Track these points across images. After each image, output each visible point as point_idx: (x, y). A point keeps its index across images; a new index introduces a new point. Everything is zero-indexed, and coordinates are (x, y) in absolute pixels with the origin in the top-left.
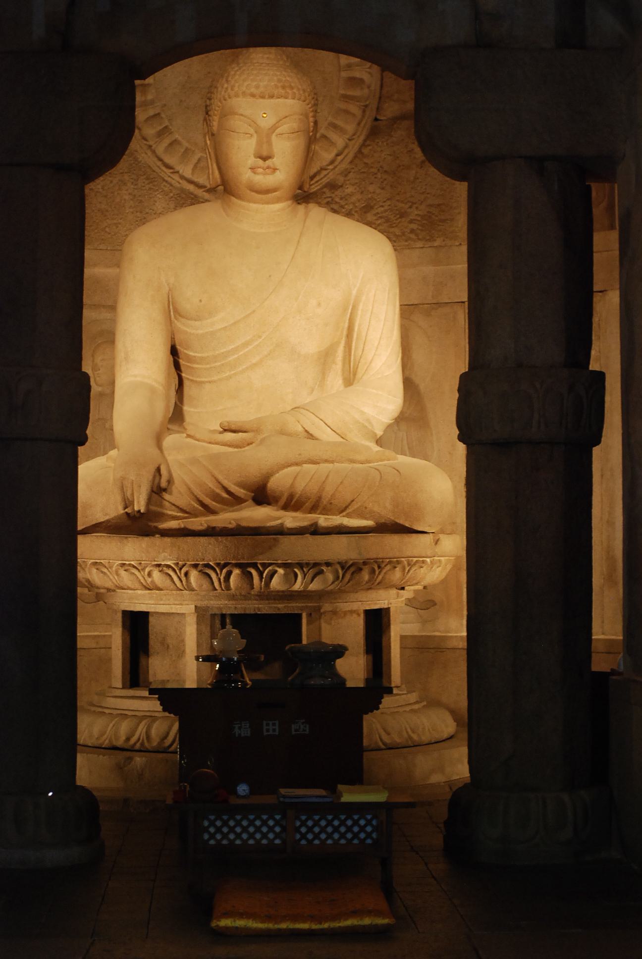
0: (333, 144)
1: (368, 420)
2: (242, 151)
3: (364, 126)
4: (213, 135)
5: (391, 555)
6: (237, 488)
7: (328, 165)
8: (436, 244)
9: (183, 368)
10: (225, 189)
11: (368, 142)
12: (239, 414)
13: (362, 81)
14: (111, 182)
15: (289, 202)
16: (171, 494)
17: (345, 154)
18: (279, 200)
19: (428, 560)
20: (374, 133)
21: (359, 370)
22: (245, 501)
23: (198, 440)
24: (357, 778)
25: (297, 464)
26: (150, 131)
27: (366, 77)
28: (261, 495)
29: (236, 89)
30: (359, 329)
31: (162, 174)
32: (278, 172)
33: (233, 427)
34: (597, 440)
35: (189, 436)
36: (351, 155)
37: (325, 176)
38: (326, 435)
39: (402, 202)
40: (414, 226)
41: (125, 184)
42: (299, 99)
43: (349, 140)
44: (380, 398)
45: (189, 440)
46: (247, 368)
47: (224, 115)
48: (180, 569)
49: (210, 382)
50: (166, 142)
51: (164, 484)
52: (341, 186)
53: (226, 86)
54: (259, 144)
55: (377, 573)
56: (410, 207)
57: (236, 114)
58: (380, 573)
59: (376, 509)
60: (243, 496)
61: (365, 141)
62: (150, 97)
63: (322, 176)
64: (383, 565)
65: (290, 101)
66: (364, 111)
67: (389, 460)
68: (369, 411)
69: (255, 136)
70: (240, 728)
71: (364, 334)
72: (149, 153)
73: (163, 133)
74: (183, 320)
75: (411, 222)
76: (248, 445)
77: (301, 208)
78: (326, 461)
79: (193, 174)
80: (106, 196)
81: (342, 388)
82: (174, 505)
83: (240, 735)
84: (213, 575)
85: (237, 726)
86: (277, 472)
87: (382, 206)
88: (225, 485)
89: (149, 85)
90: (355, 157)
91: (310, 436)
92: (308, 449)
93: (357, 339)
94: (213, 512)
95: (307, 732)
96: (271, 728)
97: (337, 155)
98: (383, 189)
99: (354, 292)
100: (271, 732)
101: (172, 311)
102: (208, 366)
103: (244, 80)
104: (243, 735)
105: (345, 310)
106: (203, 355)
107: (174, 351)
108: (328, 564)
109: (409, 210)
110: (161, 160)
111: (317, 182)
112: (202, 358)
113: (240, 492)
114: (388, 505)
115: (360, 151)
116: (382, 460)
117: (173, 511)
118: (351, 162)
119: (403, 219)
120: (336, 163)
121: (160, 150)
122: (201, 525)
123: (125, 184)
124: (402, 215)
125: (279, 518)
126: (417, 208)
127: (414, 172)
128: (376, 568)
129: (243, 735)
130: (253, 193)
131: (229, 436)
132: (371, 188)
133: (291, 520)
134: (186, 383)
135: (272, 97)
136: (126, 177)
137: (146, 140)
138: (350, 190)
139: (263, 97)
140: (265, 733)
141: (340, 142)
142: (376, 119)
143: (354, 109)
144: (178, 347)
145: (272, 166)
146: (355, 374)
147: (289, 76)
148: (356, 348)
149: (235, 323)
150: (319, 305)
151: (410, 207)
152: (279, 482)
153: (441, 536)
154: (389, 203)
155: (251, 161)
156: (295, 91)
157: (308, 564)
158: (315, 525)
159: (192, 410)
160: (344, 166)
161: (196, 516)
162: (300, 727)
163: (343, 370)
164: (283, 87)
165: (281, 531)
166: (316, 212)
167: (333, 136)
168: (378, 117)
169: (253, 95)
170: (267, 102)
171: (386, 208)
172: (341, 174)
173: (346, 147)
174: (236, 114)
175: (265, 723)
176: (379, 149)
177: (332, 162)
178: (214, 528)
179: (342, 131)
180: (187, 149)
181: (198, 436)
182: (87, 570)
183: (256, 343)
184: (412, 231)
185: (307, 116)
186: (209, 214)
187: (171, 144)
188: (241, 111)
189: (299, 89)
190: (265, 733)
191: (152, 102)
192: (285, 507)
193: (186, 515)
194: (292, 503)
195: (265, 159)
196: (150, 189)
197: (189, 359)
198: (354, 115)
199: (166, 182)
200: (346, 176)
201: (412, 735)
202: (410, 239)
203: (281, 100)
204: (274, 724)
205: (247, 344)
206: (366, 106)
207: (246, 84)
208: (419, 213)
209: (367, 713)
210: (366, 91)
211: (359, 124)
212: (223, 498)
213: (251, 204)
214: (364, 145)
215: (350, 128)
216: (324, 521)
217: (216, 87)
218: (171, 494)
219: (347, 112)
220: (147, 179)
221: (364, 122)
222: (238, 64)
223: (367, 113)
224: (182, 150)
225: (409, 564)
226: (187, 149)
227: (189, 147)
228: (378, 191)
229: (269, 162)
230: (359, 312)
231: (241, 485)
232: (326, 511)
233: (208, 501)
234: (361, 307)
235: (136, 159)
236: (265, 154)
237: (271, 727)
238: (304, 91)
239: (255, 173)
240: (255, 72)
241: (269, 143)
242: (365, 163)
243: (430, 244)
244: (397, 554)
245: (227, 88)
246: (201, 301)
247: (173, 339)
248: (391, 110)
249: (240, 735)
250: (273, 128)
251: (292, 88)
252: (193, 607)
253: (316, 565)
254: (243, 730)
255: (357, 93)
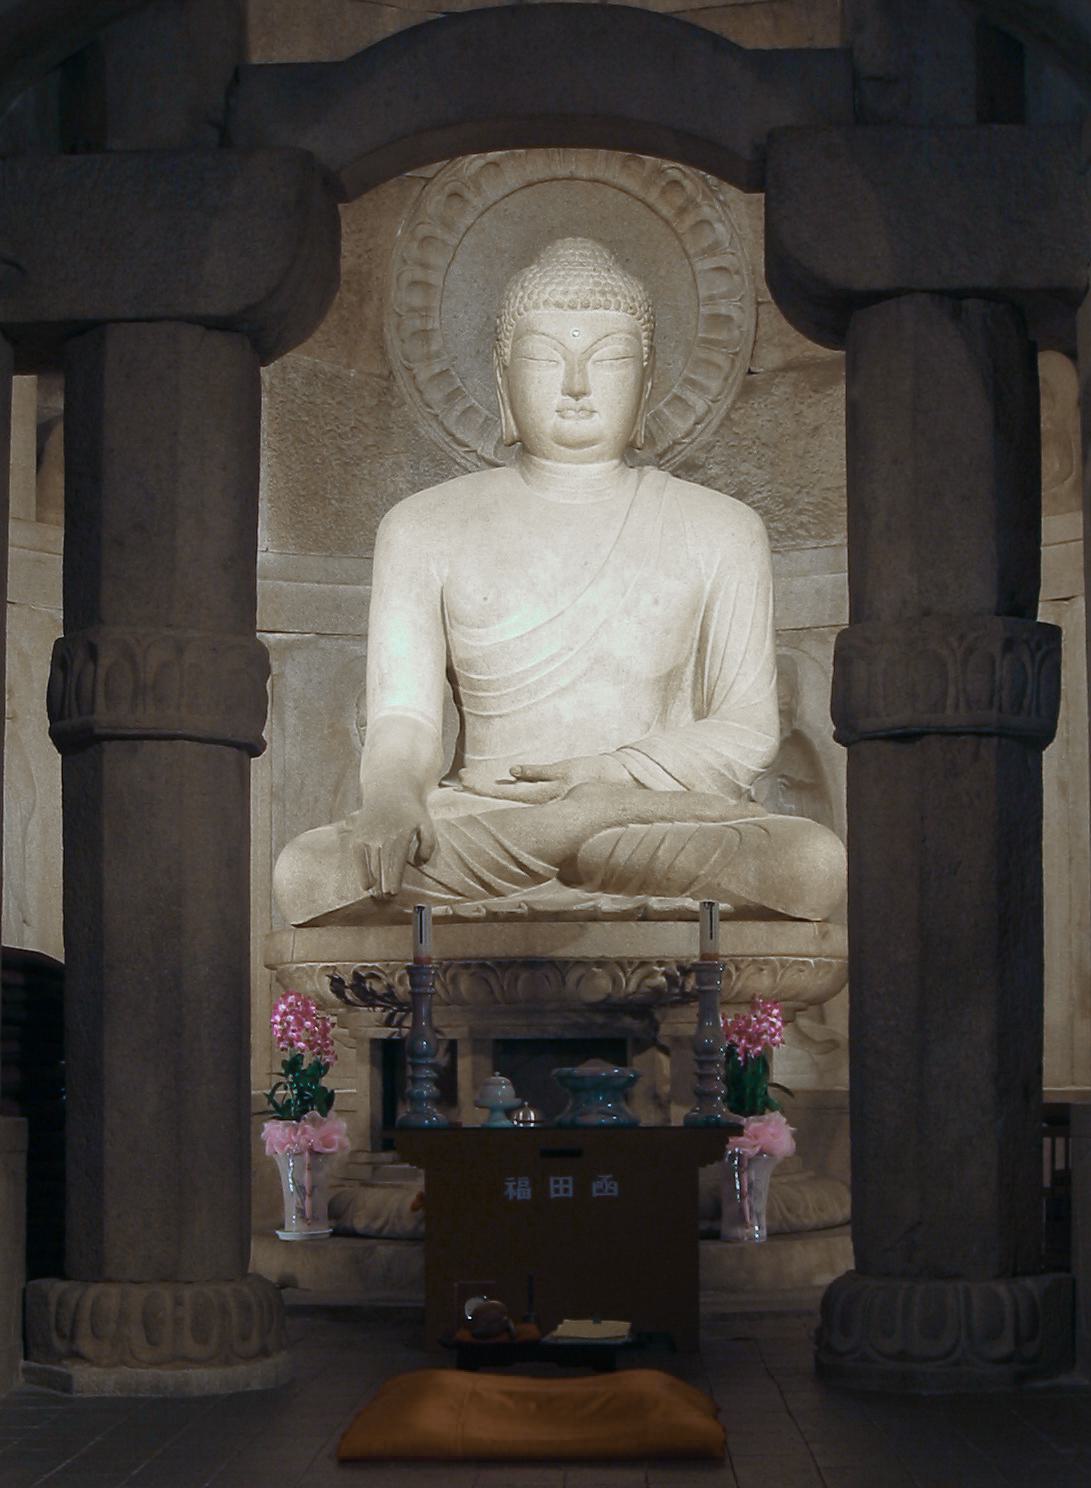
0: (689, 407)
1: (728, 766)
2: (544, 387)
3: (735, 379)
4: (505, 367)
5: (754, 950)
6: (532, 859)
7: (683, 438)
8: (835, 543)
9: (463, 701)
10: (523, 449)
11: (739, 404)
12: (535, 757)
13: (729, 319)
14: (382, 465)
15: (615, 462)
16: (434, 866)
17: (707, 420)
18: (599, 457)
19: (811, 961)
20: (747, 390)
21: (715, 696)
22: (549, 879)
23: (479, 794)
24: (429, 963)
25: (620, 824)
26: (435, 395)
27: (735, 314)
28: (570, 869)
29: (535, 297)
30: (715, 641)
31: (453, 454)
32: (596, 415)
33: (529, 773)
34: (1048, 736)
35: (466, 789)
36: (716, 422)
37: (680, 453)
38: (662, 783)
39: (788, 486)
40: (804, 518)
41: (402, 468)
42: (625, 311)
43: (713, 402)
44: (744, 735)
45: (466, 794)
46: (554, 694)
47: (518, 337)
48: (445, 972)
49: (500, 716)
50: (459, 408)
51: (424, 852)
52: (702, 466)
53: (521, 294)
54: (569, 375)
55: (734, 978)
56: (799, 492)
57: (534, 332)
58: (738, 977)
59: (733, 887)
60: (541, 872)
61: (734, 402)
62: (434, 348)
63: (675, 452)
64: (742, 966)
65: (612, 313)
66: (733, 361)
67: (754, 816)
68: (730, 753)
69: (563, 363)
70: (515, 1187)
71: (722, 645)
72: (435, 425)
73: (452, 397)
74: (462, 627)
75: (800, 512)
76: (551, 799)
77: (634, 472)
78: (663, 819)
79: (495, 454)
80: (374, 485)
81: (693, 722)
82: (441, 883)
83: (515, 1197)
84: (493, 981)
85: (510, 1185)
86: (592, 835)
87: (760, 493)
88: (514, 853)
89: (433, 330)
90: (722, 425)
91: (644, 786)
92: (637, 803)
93: (713, 652)
94: (498, 894)
95: (615, 1193)
96: (561, 1187)
97: (697, 423)
98: (760, 468)
99: (708, 587)
100: (562, 1194)
101: (445, 618)
102: (498, 693)
103: (546, 284)
104: (519, 1197)
105: (694, 612)
106: (490, 677)
107: (451, 675)
108: (660, 963)
109: (796, 498)
110: (451, 435)
111: (668, 461)
112: (488, 682)
113: (538, 865)
114: (751, 879)
115: (728, 417)
116: (745, 817)
117: (439, 891)
118: (715, 433)
119: (790, 510)
120: (695, 435)
121: (450, 422)
122: (478, 910)
123: (402, 468)
124: (788, 503)
125: (591, 900)
126: (808, 493)
127: (803, 443)
128: (733, 970)
129: (519, 1197)
130: (562, 448)
131: (524, 786)
132: (744, 467)
133: (607, 902)
134: (469, 719)
135: (586, 307)
136: (403, 458)
137: (428, 406)
138: (714, 470)
139: (573, 308)
140: (553, 1195)
141: (700, 406)
142: (750, 372)
143: (719, 358)
144: (456, 668)
145: (588, 407)
146: (709, 704)
147: (612, 278)
148: (710, 669)
149: (534, 630)
150: (656, 602)
151: (799, 492)
152: (596, 846)
153: (830, 926)
154: (769, 487)
155: (558, 399)
156: (619, 298)
157: (631, 963)
158: (645, 907)
159: (477, 758)
160: (706, 438)
161: (473, 899)
162: (605, 1186)
163: (694, 700)
164: (603, 293)
165: (595, 916)
166: (653, 475)
167: (691, 397)
168: (753, 369)
169: (558, 305)
170: (580, 313)
171: (765, 494)
172: (702, 448)
173: (709, 411)
174: (534, 332)
175: (552, 1180)
176: (755, 413)
177: (688, 435)
178: (495, 913)
179: (704, 389)
180: (487, 419)
181: (478, 787)
182: (315, 978)
183: (565, 658)
184: (802, 525)
185: (637, 336)
186: (504, 481)
187: (464, 412)
188: (542, 329)
189: (625, 297)
190: (553, 1195)
191: (438, 355)
192: (604, 887)
193: (459, 898)
194: (614, 880)
195: (576, 396)
196: (436, 474)
197: (473, 685)
198: (719, 367)
199: (458, 464)
200: (709, 451)
201: (788, 1215)
202: (799, 536)
203: (600, 312)
204: (566, 1182)
205: (551, 659)
206: (736, 354)
207: (549, 289)
208: (811, 500)
209: (704, 1166)
210: (737, 333)
211: (726, 379)
212: (513, 874)
213: (561, 465)
214: (733, 408)
215: (714, 385)
216: (655, 903)
217: (508, 299)
218: (434, 866)
219: (709, 363)
220: (432, 461)
221: (734, 375)
222: (539, 264)
223: (738, 364)
224: (481, 420)
225: (783, 966)
226: (487, 419)
227: (491, 416)
228: (754, 471)
229: (583, 401)
230: (715, 614)
231: (539, 854)
232: (660, 890)
233: (488, 877)
234: (717, 608)
235: (416, 433)
236: (577, 388)
237: (561, 1186)
238: (633, 300)
239: (563, 417)
240: (562, 273)
241: (584, 375)
242: (737, 434)
243: (827, 543)
244: (764, 950)
245: (522, 297)
246: (485, 599)
247: (449, 657)
248: (771, 358)
249: (515, 1197)
250: (588, 353)
251: (615, 295)
252: (465, 1029)
253: (643, 963)
254: (519, 1190)
255: (723, 336)
